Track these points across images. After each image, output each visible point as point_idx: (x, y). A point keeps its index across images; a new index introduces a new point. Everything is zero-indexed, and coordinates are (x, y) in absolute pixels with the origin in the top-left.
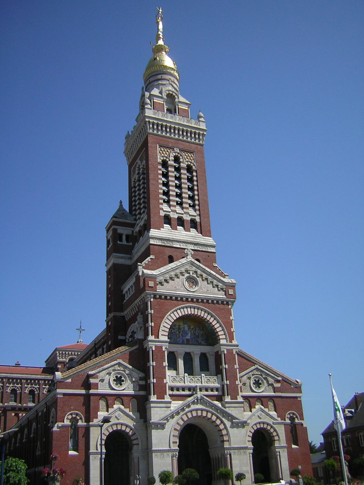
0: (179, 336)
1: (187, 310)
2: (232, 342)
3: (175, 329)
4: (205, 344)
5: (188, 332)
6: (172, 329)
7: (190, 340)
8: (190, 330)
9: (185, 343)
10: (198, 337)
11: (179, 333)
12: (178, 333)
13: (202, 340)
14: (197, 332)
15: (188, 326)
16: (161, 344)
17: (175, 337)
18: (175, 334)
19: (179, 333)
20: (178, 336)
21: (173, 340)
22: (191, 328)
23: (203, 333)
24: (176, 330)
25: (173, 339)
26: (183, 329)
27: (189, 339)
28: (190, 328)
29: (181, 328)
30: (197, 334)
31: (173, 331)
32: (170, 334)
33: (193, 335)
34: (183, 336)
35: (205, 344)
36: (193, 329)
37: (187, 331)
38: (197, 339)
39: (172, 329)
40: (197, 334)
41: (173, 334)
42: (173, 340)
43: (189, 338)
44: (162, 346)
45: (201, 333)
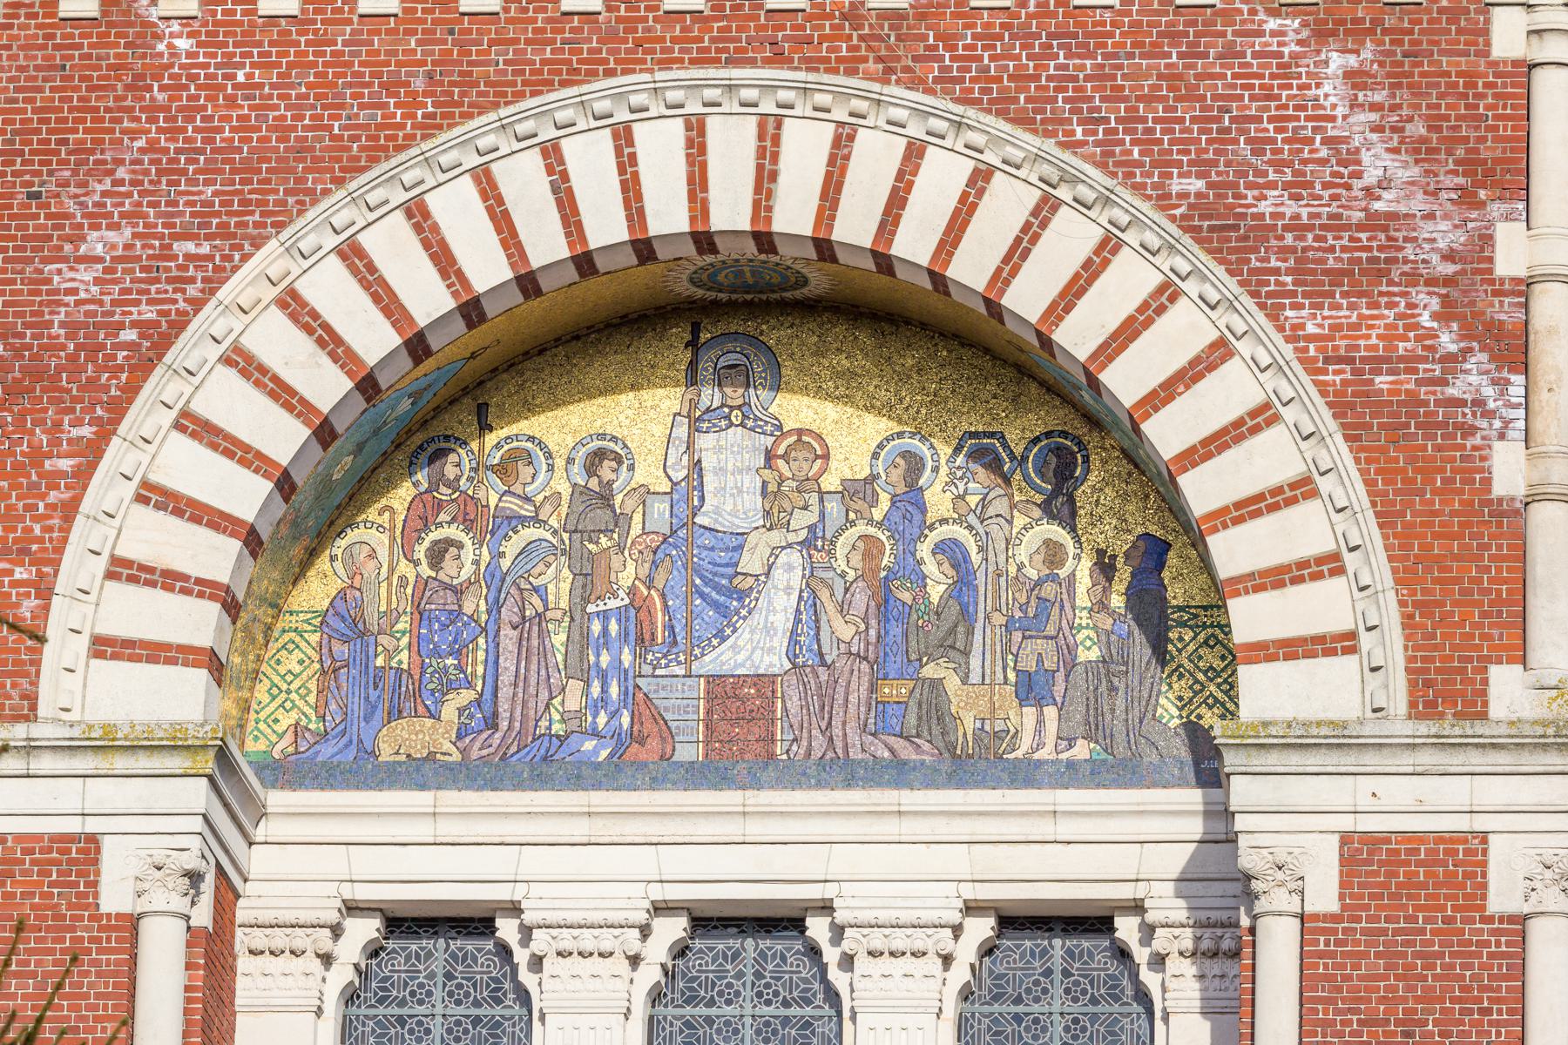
0: (581, 641)
1: (627, 164)
2: (1475, 706)
3: (523, 520)
4: (1081, 750)
5: (751, 562)
6: (454, 532)
7: (791, 701)
8: (802, 520)
9: (688, 752)
10: (953, 647)
11: (589, 581)
12: (559, 583)
13: (1030, 689)
14: (939, 548)
15: (769, 456)
16: (68, 795)
17: (508, 663)
18: (509, 613)
19: (589, 581)
20: (559, 639)
21: (449, 712)
22: (830, 482)
23: (1053, 555)
24: (530, 533)
25: (467, 696)
26: (660, 508)
27: (763, 681)
28: (808, 483)
29: (645, 494)
30: (936, 592)
31: (467, 562)
32: (420, 613)
33: (860, 600)
34: (643, 642)
35: (1081, 750)
36: (858, 491)
37: (737, 544)
38: (929, 671)
39: (454, 532)
40: (936, 592)
41: (475, 604)
42: (449, 712)
43: (775, 662)
44: (93, 839)
45: (1022, 554)
